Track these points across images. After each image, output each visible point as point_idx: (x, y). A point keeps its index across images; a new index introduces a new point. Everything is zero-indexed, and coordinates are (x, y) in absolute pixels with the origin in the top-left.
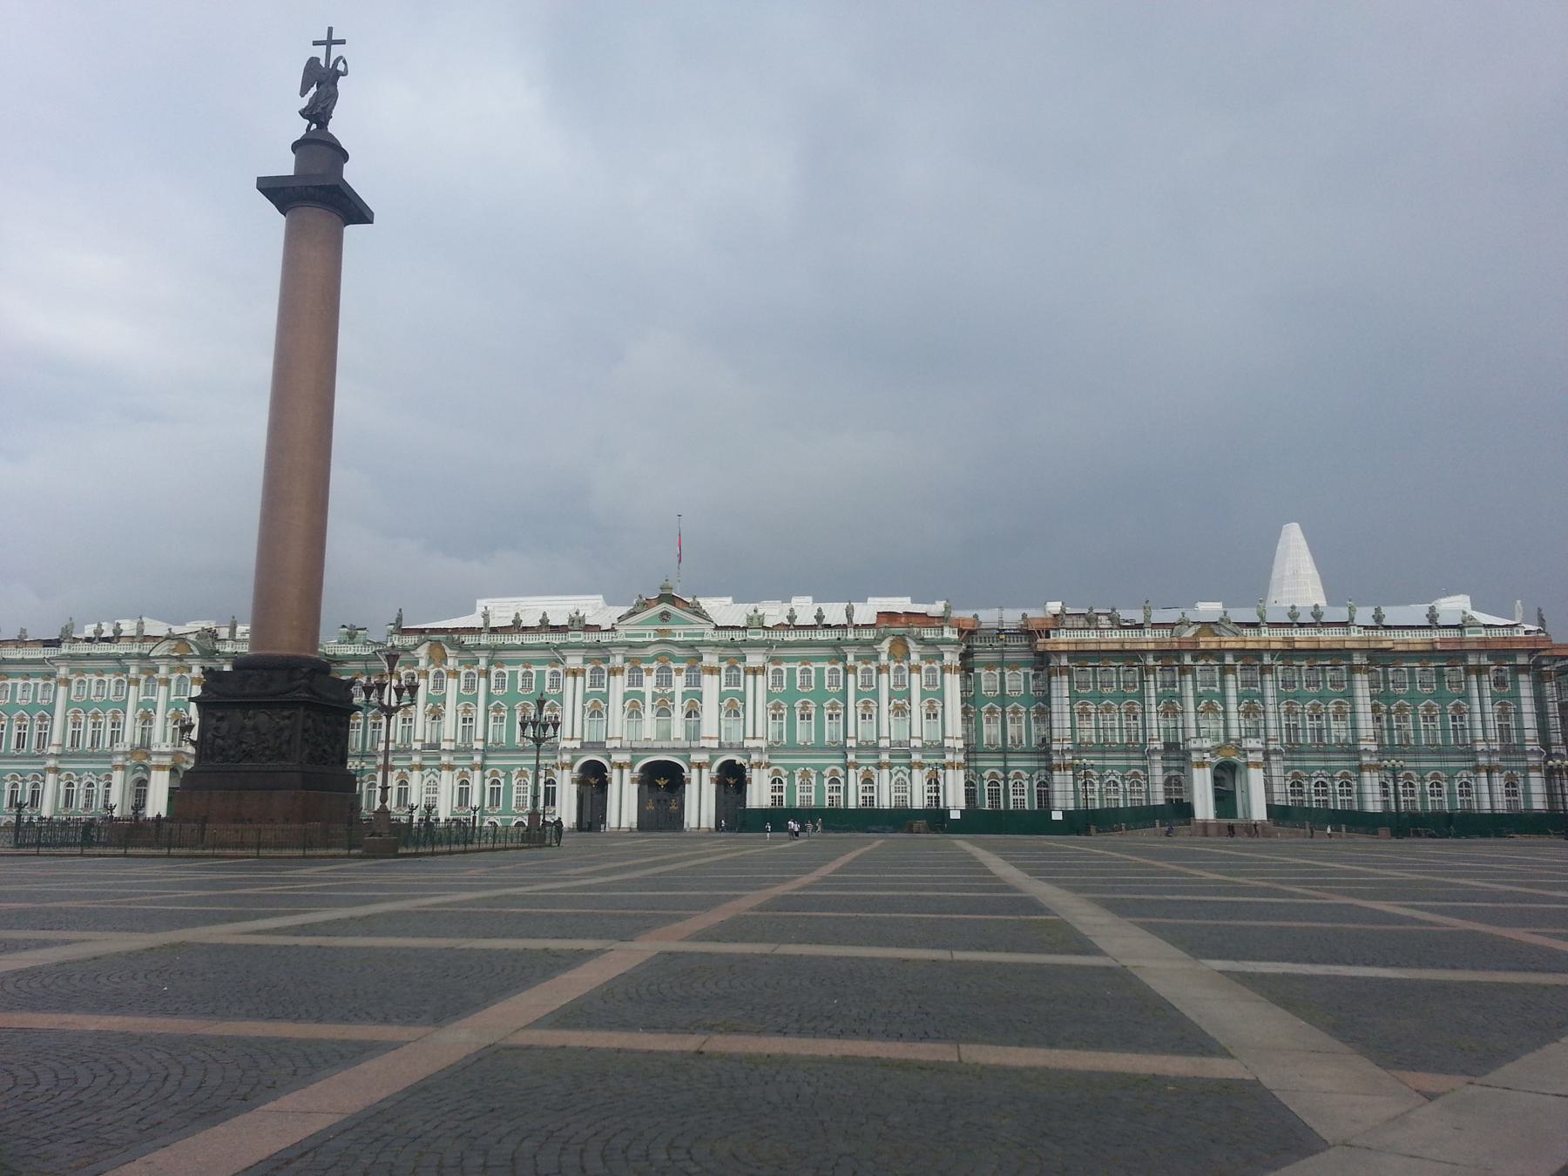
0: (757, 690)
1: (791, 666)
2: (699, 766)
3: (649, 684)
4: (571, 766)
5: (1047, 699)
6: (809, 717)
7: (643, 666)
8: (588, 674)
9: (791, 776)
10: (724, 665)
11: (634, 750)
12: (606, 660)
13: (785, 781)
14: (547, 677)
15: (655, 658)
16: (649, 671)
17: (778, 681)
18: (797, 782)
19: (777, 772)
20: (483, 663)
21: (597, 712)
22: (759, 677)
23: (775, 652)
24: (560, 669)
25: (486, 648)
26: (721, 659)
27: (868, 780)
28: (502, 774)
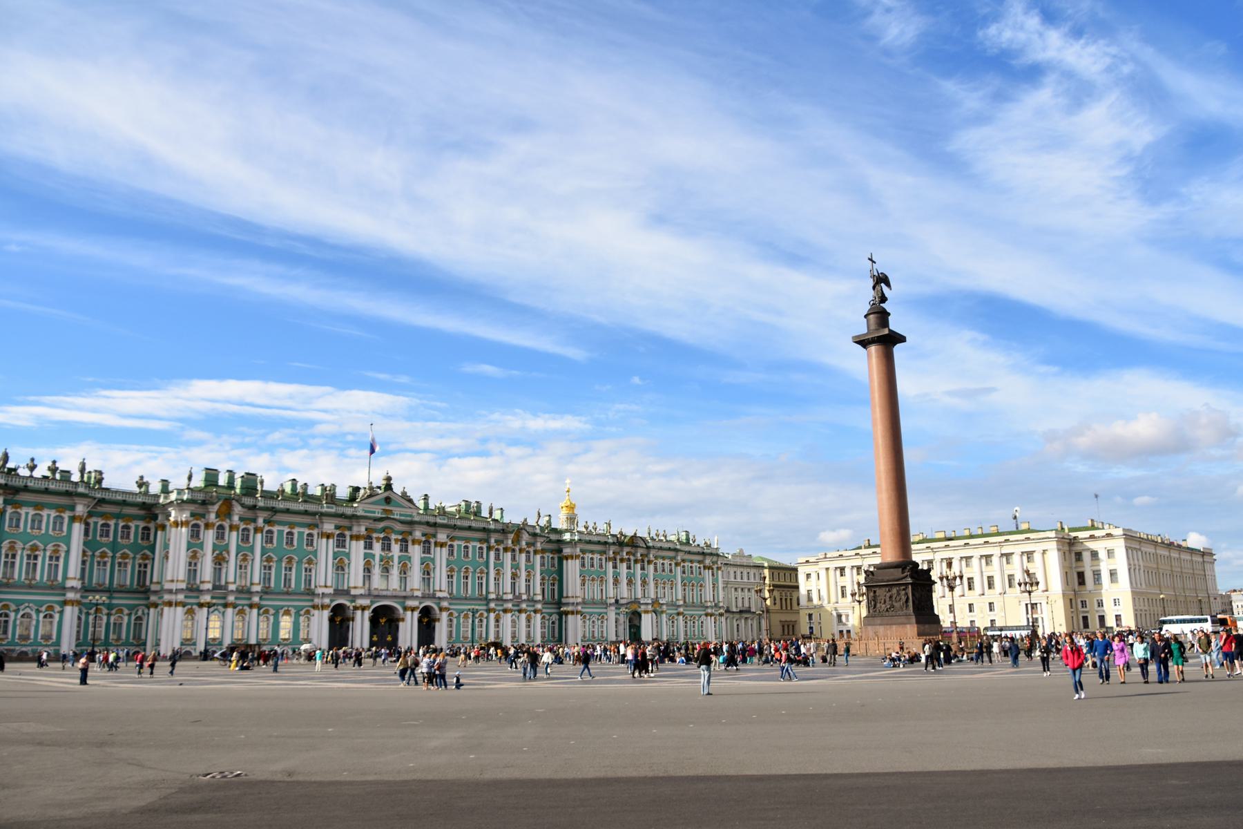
0: (440, 555)
2: (413, 610)
5: (560, 572)
7: (375, 535)
9: (458, 618)
12: (350, 529)
13: (455, 621)
16: (378, 539)
17: (451, 553)
19: (451, 614)
20: (260, 521)
21: (340, 567)
24: (315, 532)
25: (262, 509)
26: (424, 535)
27: (497, 621)
28: (272, 611)
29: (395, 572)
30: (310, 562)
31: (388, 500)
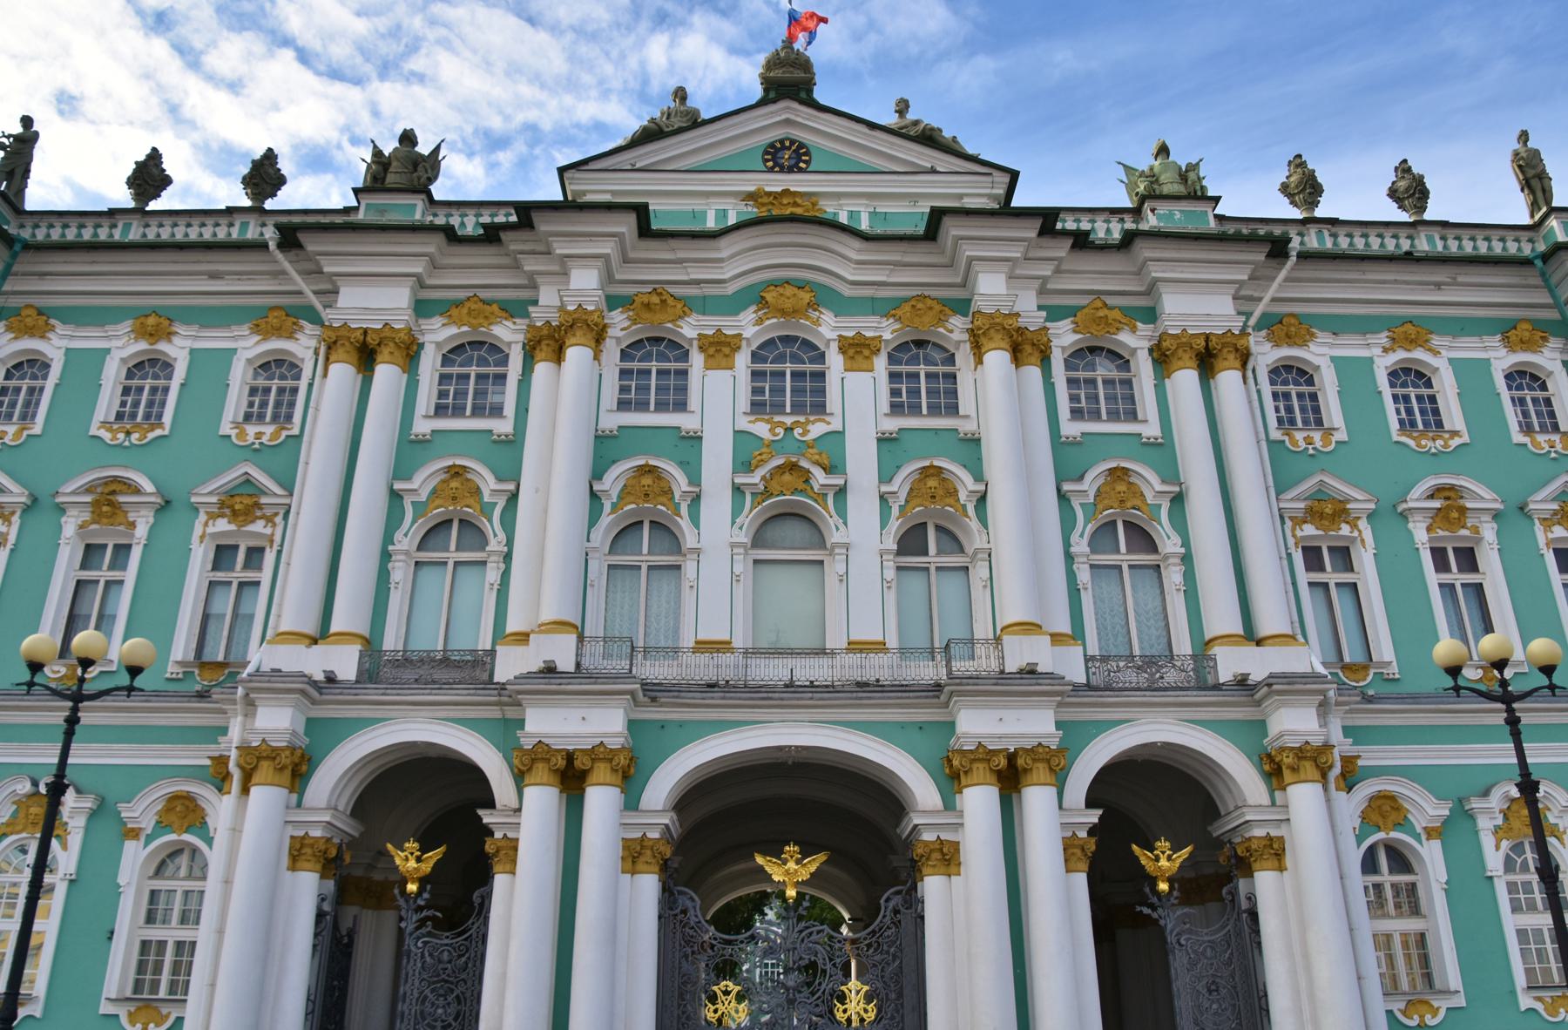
1: (1351, 348)
2: (1010, 775)
3: (719, 400)
4: (296, 768)
6: (1468, 560)
8: (429, 364)
10: (1064, 337)
11: (653, 692)
13: (1432, 858)
14: (239, 376)
15: (756, 297)
16: (719, 349)
18: (1494, 860)
19: (1384, 809)
22: (1228, 381)
23: (1280, 287)
24: (303, 346)
29: (863, 531)
30: (242, 503)
31: (787, 155)
